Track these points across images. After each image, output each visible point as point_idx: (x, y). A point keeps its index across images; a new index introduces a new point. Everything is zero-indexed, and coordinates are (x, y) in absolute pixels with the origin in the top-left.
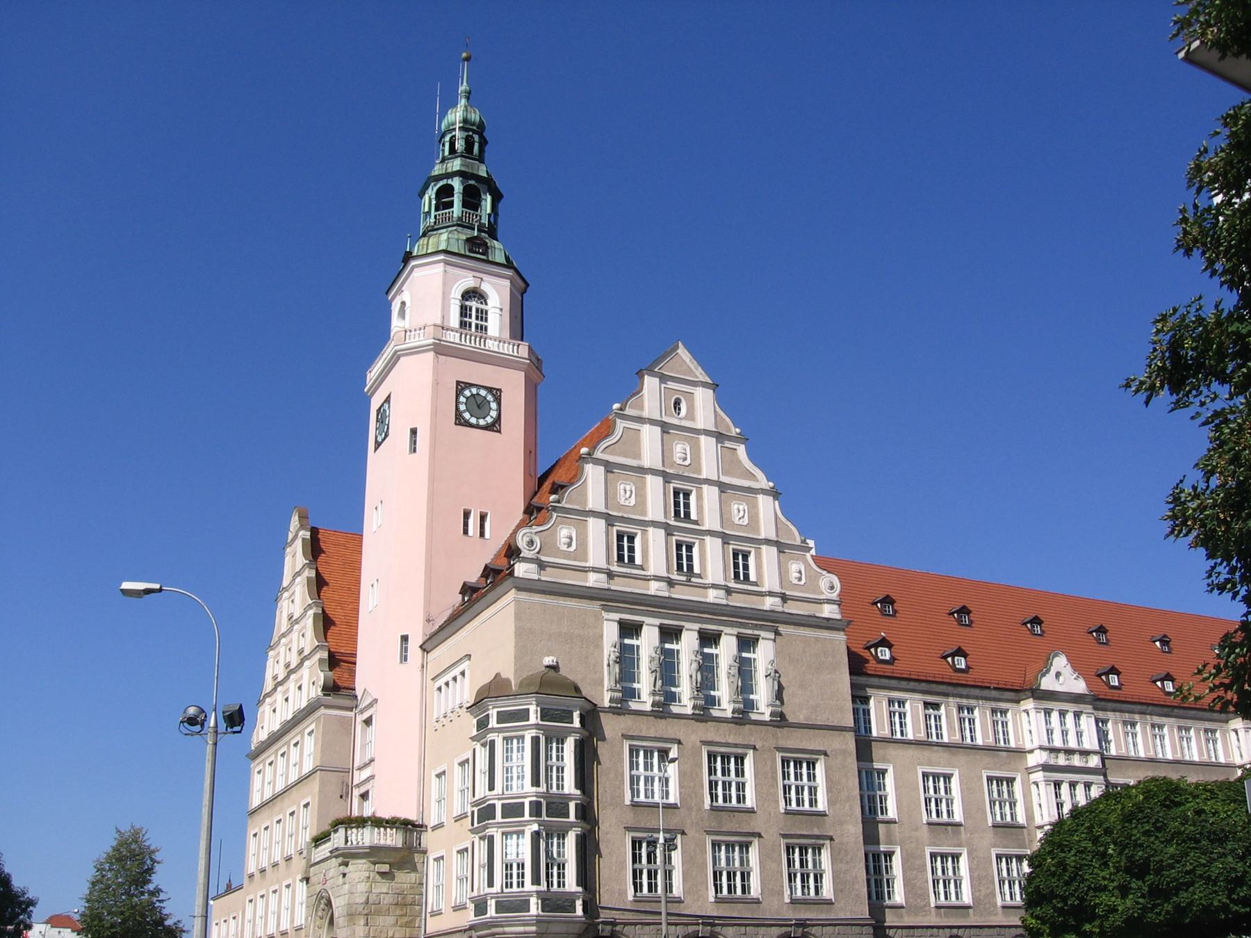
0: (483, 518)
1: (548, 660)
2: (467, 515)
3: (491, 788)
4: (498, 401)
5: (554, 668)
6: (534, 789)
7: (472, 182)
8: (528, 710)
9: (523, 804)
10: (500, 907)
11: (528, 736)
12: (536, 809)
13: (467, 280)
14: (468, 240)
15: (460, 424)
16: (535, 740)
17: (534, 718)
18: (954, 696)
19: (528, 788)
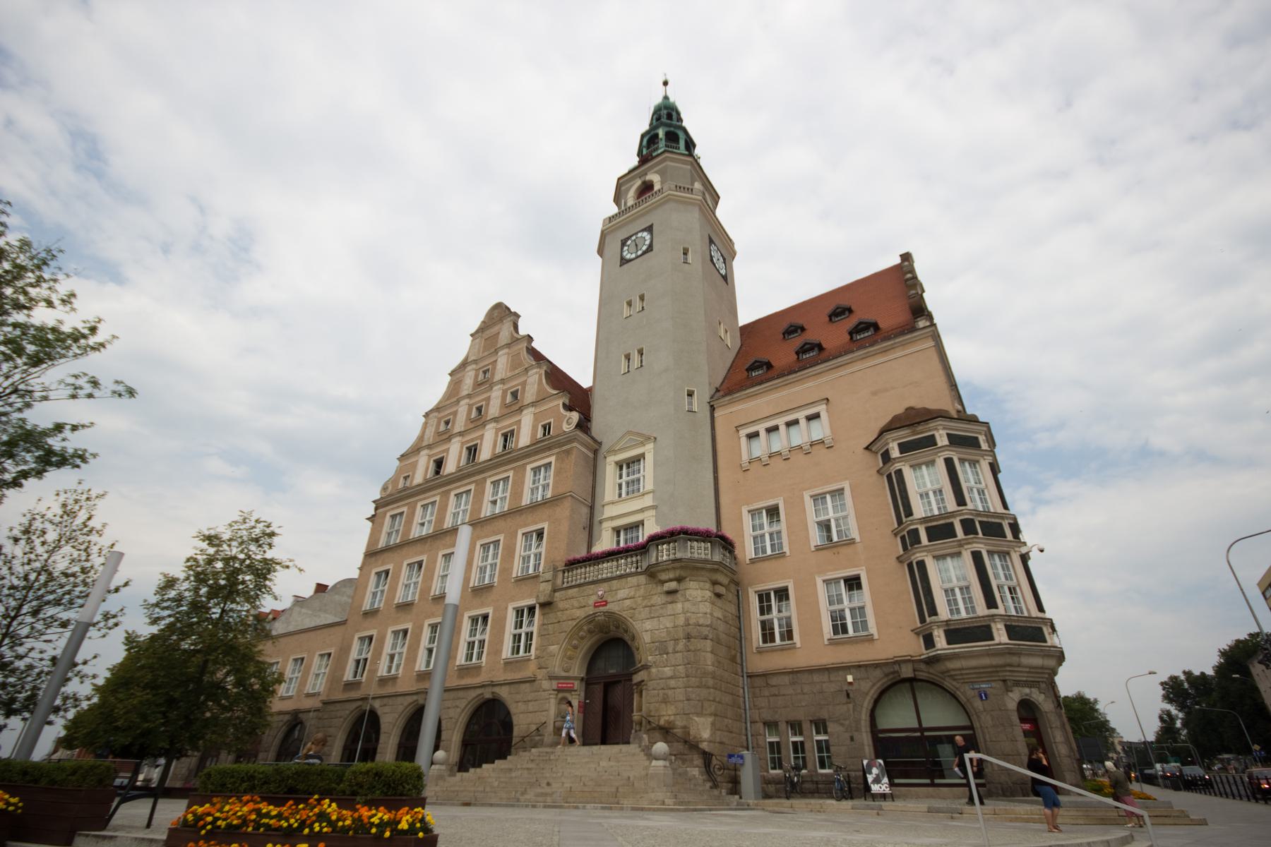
3: (961, 501)
10: (1012, 631)
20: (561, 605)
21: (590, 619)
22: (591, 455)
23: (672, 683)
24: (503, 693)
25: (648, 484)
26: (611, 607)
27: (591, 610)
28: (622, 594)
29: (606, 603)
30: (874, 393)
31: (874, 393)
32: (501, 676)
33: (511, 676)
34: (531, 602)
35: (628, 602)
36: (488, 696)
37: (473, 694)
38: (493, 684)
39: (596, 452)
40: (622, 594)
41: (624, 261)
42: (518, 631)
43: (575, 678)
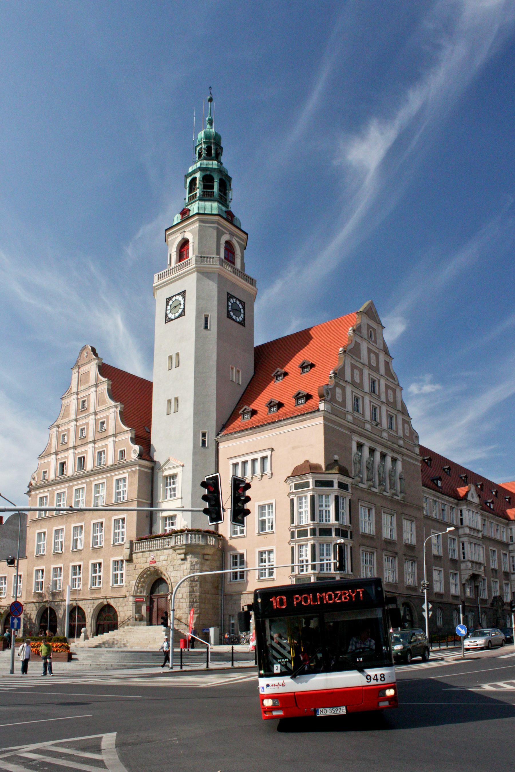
0: (238, 371)
1: (336, 457)
2: (232, 368)
4: (244, 308)
5: (336, 461)
6: (312, 522)
7: (224, 178)
8: (309, 482)
9: (307, 530)
11: (309, 494)
12: (313, 532)
13: (225, 237)
14: (226, 212)
15: (229, 318)
16: (337, 498)
17: (336, 486)
18: (442, 499)
19: (309, 522)
20: (135, 561)
21: (148, 569)
22: (149, 471)
23: (181, 600)
24: (112, 602)
25: (179, 494)
26: (157, 565)
27: (148, 565)
28: (162, 558)
29: (155, 562)
30: (293, 448)
31: (293, 448)
32: (110, 595)
33: (115, 595)
34: (121, 558)
35: (164, 562)
36: (105, 603)
37: (97, 602)
38: (106, 598)
39: (152, 469)
40: (162, 558)
41: (168, 320)
42: (116, 572)
43: (144, 596)
